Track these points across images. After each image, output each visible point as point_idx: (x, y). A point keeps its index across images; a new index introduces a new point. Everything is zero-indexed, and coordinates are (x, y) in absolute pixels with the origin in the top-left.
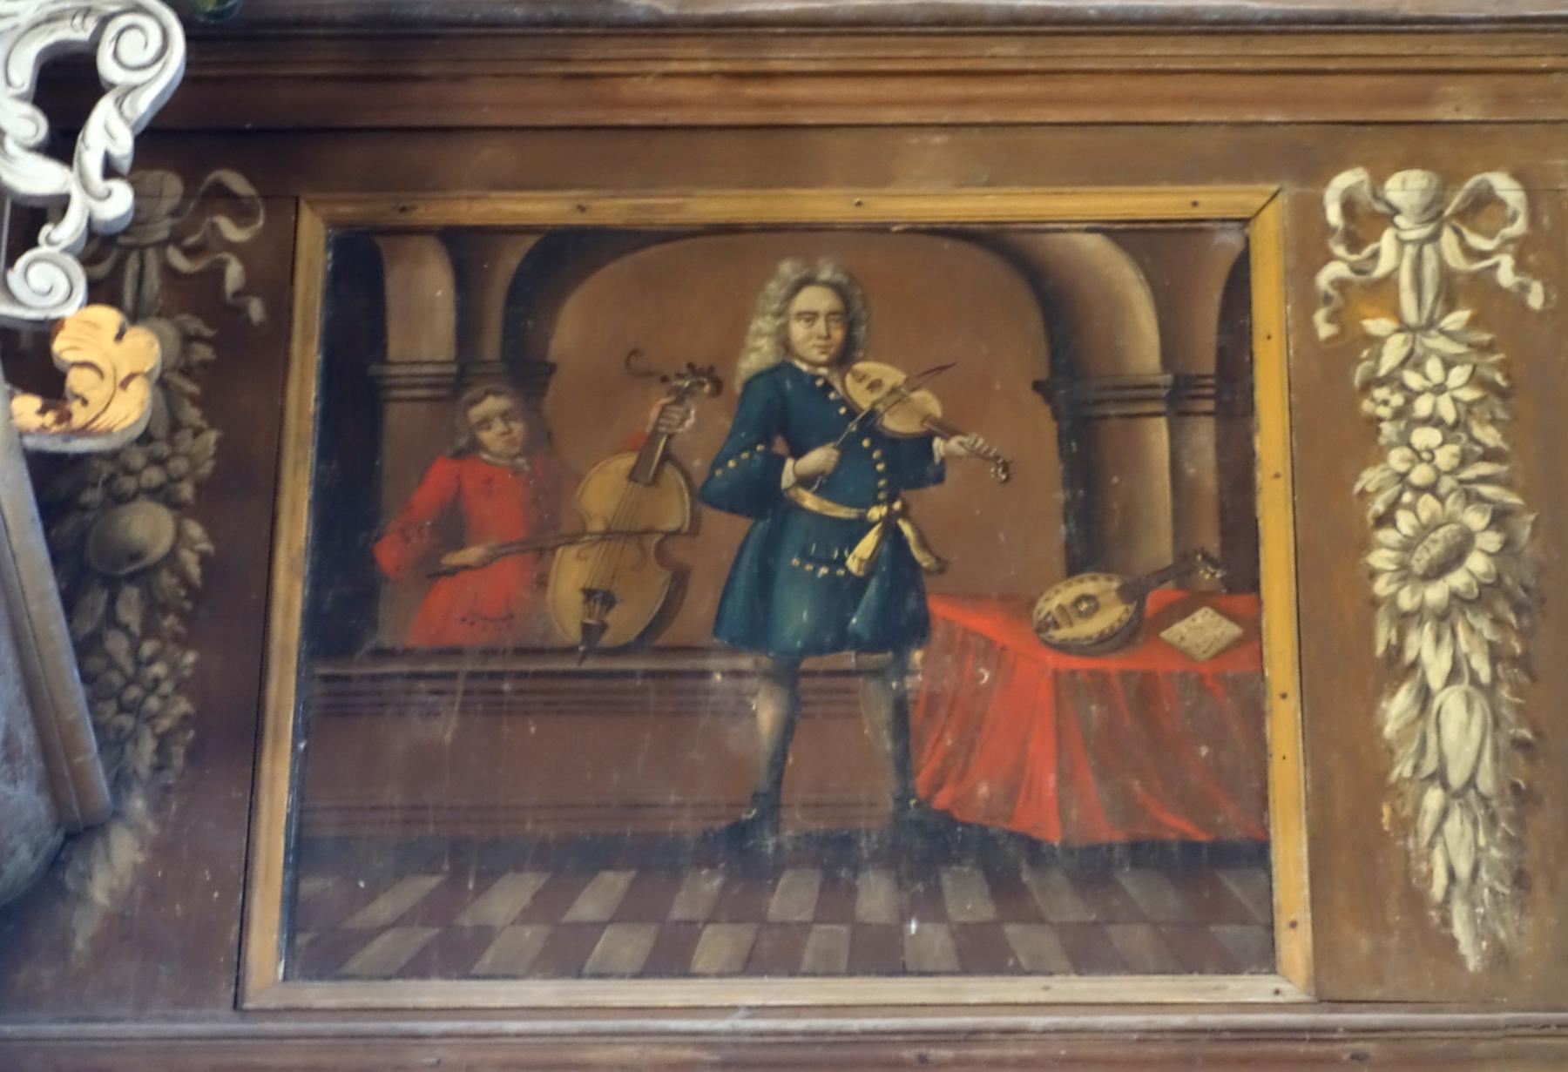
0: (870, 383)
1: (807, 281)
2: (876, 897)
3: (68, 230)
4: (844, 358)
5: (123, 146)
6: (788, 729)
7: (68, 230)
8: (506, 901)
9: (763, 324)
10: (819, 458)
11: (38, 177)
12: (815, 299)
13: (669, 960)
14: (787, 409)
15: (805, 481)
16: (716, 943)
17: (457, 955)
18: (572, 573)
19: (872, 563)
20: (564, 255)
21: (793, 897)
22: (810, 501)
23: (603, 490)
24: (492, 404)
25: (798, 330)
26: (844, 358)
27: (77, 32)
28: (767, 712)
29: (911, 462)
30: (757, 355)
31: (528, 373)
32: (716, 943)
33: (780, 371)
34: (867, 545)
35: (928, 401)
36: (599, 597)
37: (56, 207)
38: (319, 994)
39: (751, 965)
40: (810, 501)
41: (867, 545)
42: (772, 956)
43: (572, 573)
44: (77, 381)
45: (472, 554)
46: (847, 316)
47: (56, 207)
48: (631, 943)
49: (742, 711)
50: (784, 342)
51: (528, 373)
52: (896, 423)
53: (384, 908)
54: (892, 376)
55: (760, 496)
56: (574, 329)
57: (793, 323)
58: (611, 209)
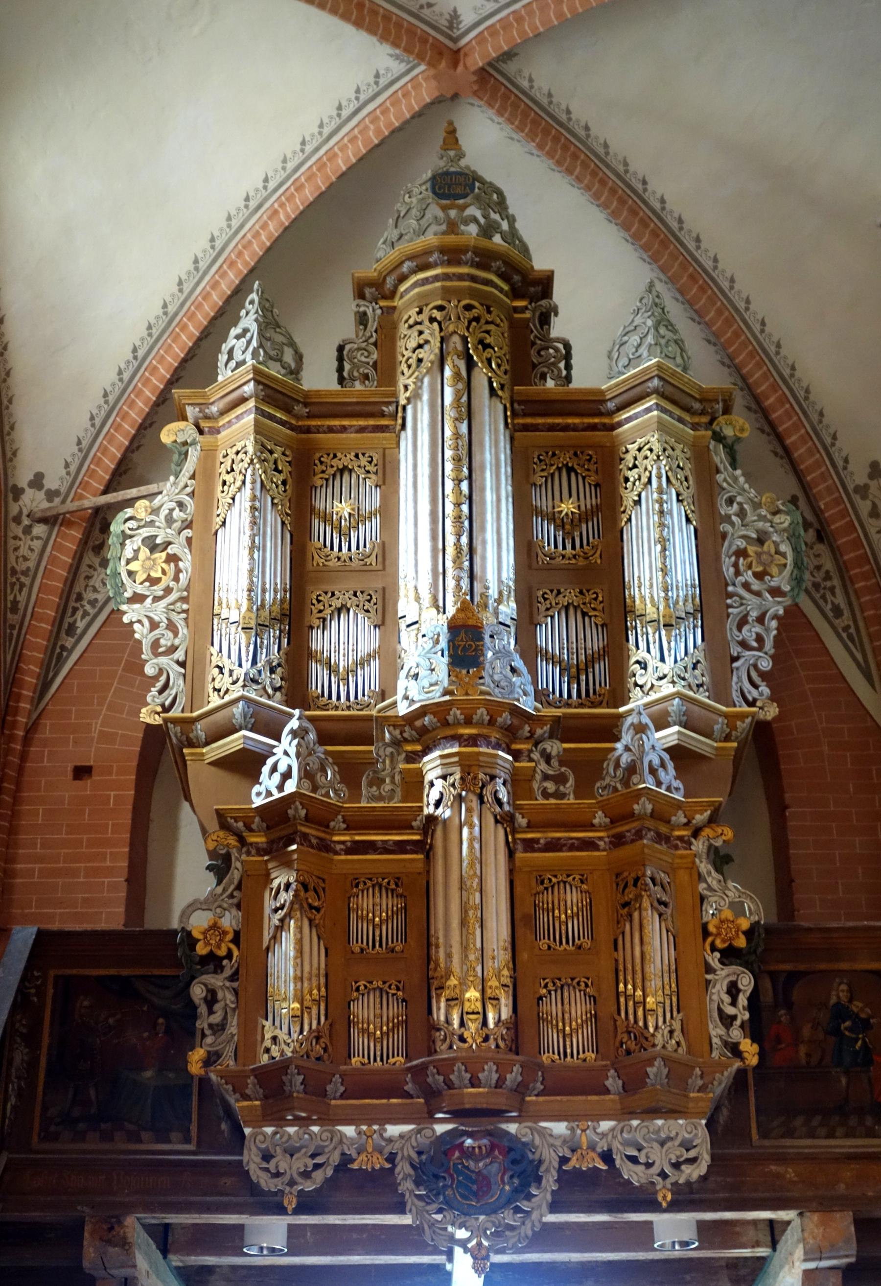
0: (856, 1006)
1: (840, 984)
2: (869, 1121)
3: (738, 1022)
4: (851, 1001)
5: (746, 1003)
6: (848, 1083)
7: (738, 1022)
8: (799, 1121)
9: (834, 993)
10: (848, 1023)
11: (730, 1010)
12: (844, 987)
13: (831, 1135)
14: (841, 1012)
15: (846, 1029)
16: (840, 1131)
17: (790, 1133)
18: (803, 1050)
19: (861, 1048)
20: (793, 977)
21: (853, 1121)
22: (847, 1033)
23: (806, 1031)
24: (782, 1012)
25: (841, 994)
26: (851, 1001)
27: (733, 978)
28: (844, 1081)
29: (865, 1025)
30: (833, 1000)
31: (789, 1005)
32: (840, 1131)
33: (838, 1004)
34: (860, 1043)
35: (868, 1010)
36: (808, 1055)
37: (734, 1018)
38: (767, 1142)
39: (847, 1136)
40: (847, 1033)
41: (860, 1043)
42: (850, 1134)
43: (803, 1050)
44: (746, 1055)
45: (783, 1046)
46: (850, 991)
47: (734, 1018)
48: (823, 1131)
49: (840, 1081)
50: (838, 997)
51: (789, 1005)
52: (863, 1016)
53: (775, 1123)
54: (860, 1005)
55: (836, 1032)
56: (796, 995)
57: (840, 992)
58: (802, 967)
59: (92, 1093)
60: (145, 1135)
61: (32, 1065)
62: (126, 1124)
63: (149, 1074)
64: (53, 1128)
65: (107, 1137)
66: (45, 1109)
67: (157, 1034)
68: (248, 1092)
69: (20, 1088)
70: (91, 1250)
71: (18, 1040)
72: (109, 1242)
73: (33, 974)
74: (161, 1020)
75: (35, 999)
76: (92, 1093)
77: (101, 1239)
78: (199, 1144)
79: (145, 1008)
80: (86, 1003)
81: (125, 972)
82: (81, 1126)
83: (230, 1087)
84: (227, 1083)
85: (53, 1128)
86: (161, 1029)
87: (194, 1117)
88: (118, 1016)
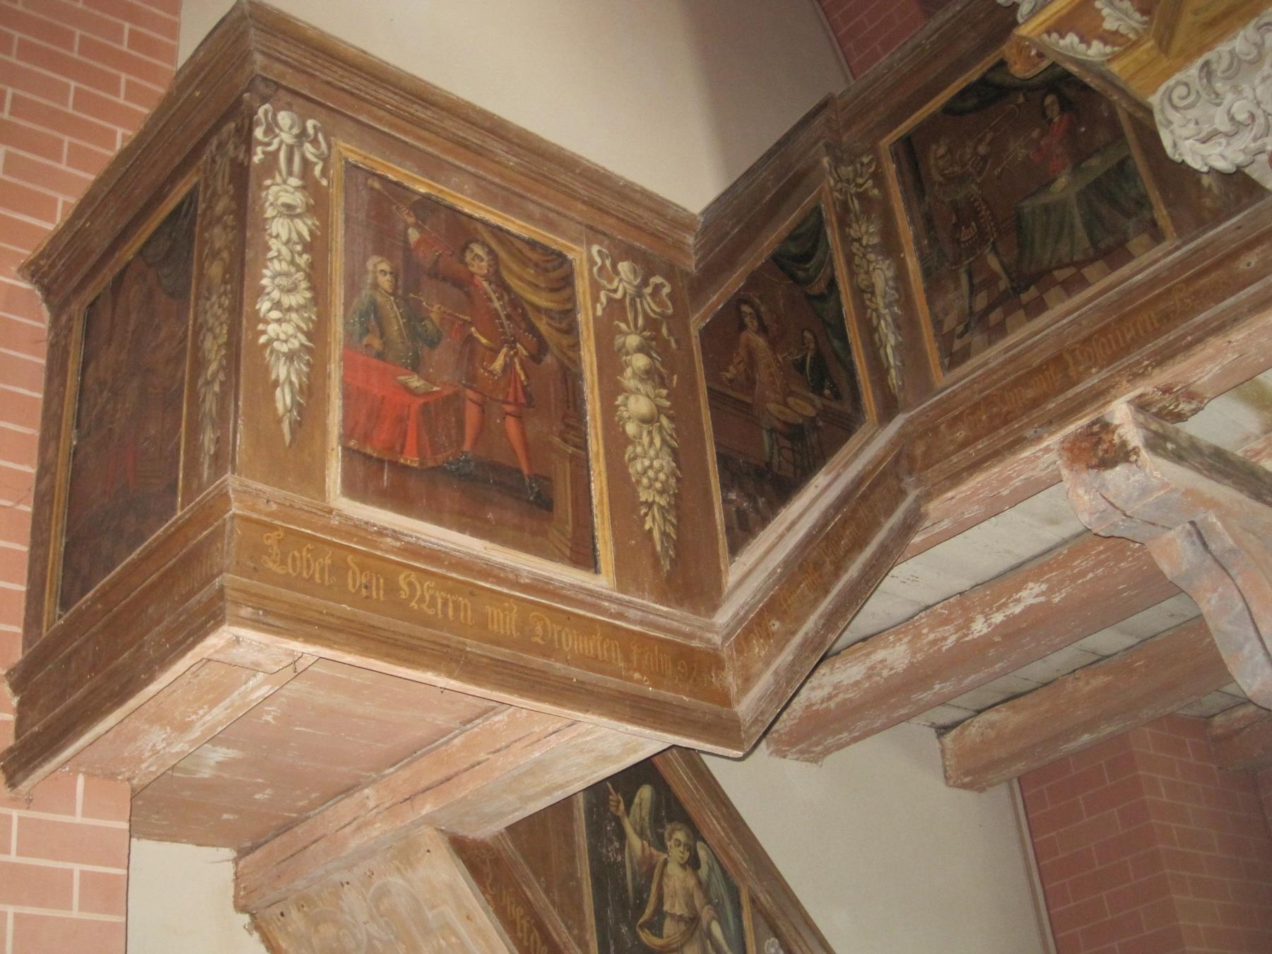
59: (994, 263)
60: (1088, 272)
61: (901, 276)
62: (1056, 273)
63: (1062, 181)
64: (958, 344)
65: (1037, 308)
66: (937, 323)
67: (1051, 121)
68: (1109, 25)
69: (895, 318)
70: (1081, 491)
71: (872, 257)
72: (1106, 463)
73: (862, 164)
74: (1049, 99)
75: (876, 192)
76: (994, 263)
77: (1090, 467)
78: (1179, 230)
79: (1021, 99)
80: (942, 151)
81: (973, 75)
82: (995, 317)
83: (1072, 39)
84: (1062, 36)
85: (958, 344)
86: (1054, 113)
87: (1154, 196)
88: (989, 136)
